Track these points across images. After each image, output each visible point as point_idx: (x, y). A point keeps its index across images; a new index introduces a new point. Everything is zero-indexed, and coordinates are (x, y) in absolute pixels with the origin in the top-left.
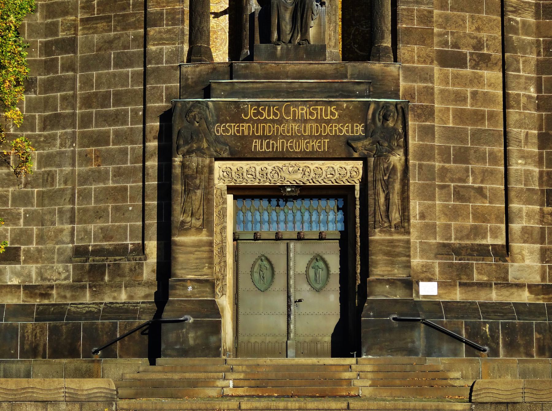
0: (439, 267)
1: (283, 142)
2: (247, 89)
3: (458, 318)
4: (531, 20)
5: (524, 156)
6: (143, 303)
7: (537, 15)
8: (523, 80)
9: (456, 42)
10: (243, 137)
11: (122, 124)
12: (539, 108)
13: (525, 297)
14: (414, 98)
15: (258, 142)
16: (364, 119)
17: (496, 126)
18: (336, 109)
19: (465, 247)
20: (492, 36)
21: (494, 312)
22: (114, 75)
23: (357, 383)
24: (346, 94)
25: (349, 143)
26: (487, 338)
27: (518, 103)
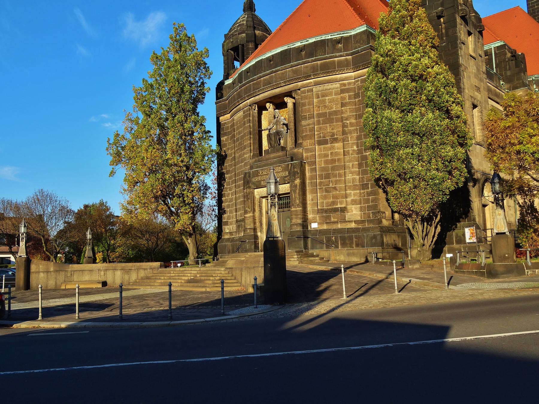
4: (353, 121)
12: (358, 153)
13: (353, 225)
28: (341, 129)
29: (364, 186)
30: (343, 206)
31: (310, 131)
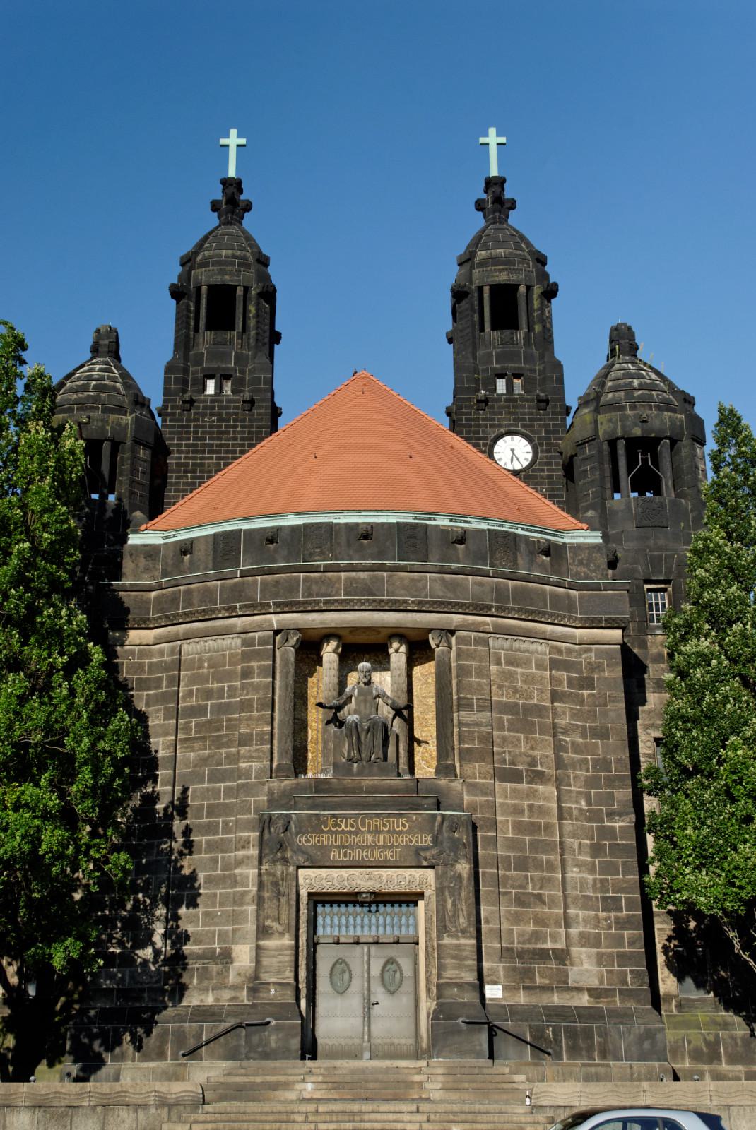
1: (359, 852)
2: (327, 802)
3: (521, 1021)
5: (579, 865)
6: (228, 1005)
7: (584, 736)
8: (574, 795)
10: (323, 846)
11: (214, 835)
12: (589, 820)
13: (585, 1000)
15: (337, 851)
16: (432, 831)
18: (407, 821)
21: (556, 1015)
22: (208, 789)
23: (428, 1086)
25: (418, 851)
26: (551, 1042)
27: (571, 815)
28: (550, 752)
29: (610, 904)
31: (480, 741)
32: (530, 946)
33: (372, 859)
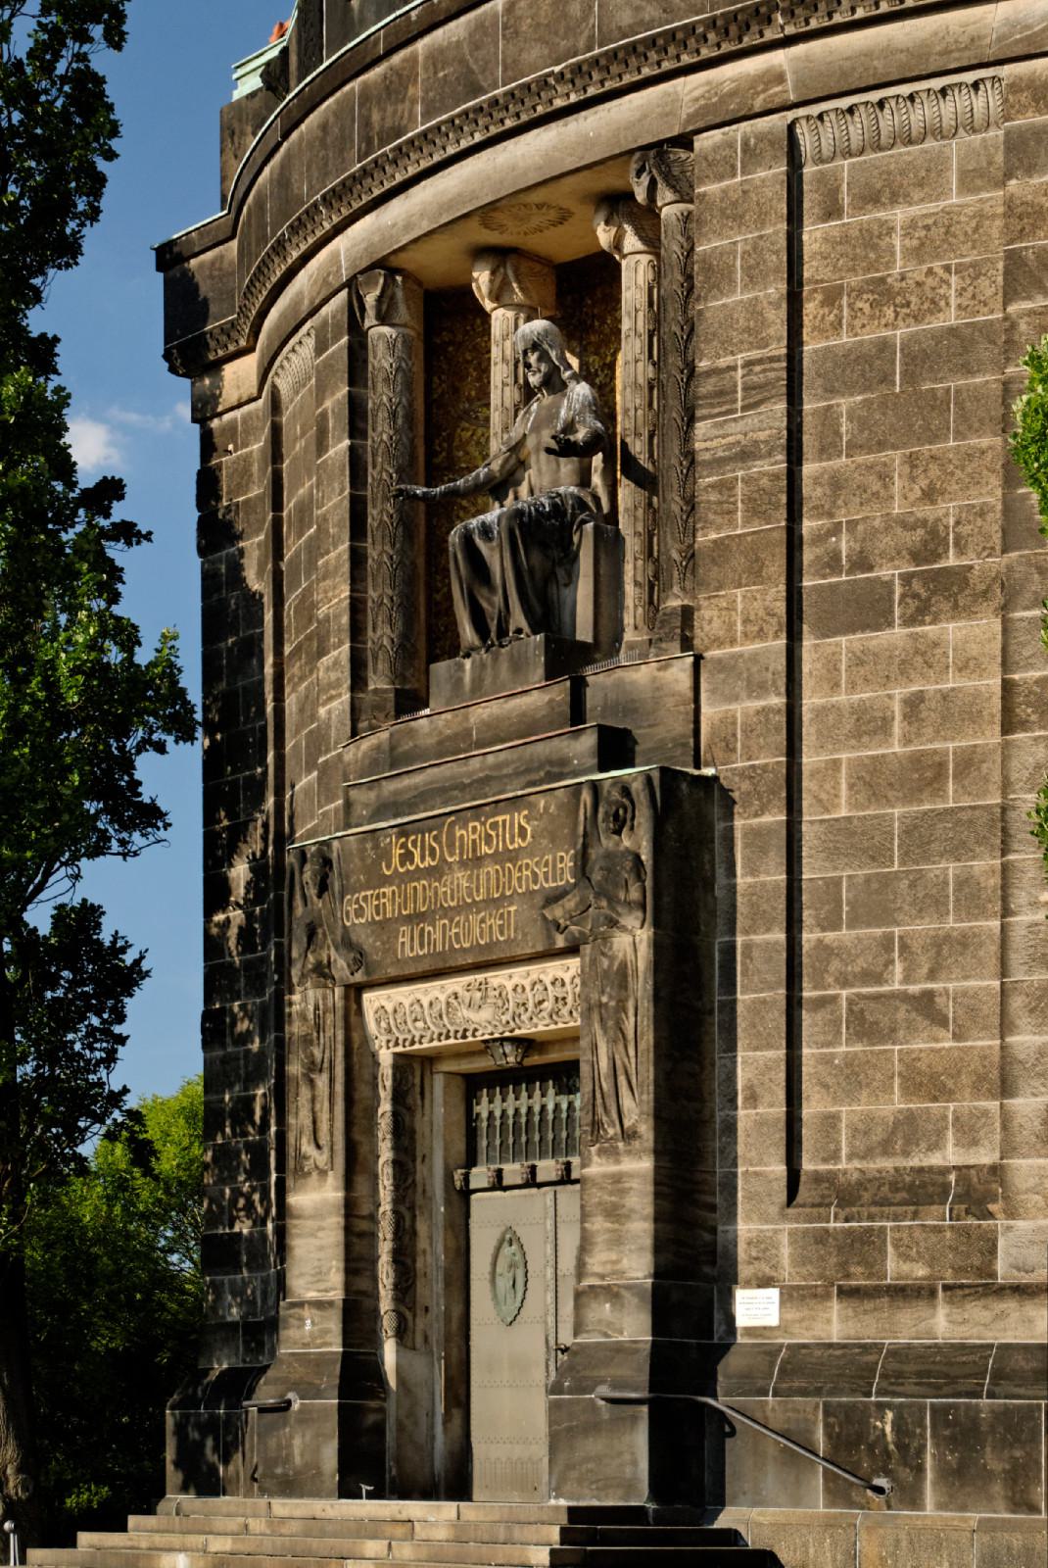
0: (791, 1244)
9: (861, 552)
10: (386, 921)
14: (734, 750)
17: (985, 793)
19: (876, 1179)
20: (973, 506)
24: (556, 770)
26: (888, 1454)
30: (985, 1156)
32: (886, 1164)
33: (466, 945)
